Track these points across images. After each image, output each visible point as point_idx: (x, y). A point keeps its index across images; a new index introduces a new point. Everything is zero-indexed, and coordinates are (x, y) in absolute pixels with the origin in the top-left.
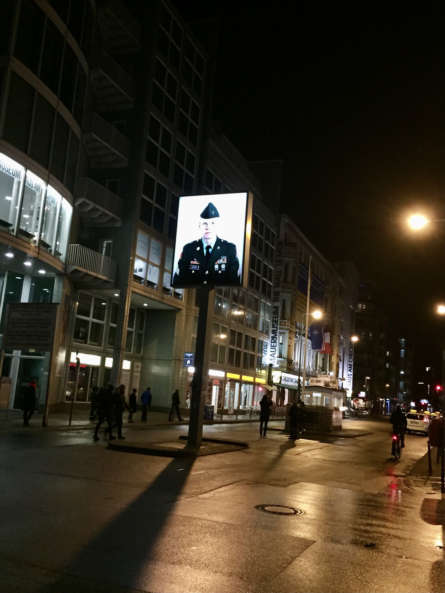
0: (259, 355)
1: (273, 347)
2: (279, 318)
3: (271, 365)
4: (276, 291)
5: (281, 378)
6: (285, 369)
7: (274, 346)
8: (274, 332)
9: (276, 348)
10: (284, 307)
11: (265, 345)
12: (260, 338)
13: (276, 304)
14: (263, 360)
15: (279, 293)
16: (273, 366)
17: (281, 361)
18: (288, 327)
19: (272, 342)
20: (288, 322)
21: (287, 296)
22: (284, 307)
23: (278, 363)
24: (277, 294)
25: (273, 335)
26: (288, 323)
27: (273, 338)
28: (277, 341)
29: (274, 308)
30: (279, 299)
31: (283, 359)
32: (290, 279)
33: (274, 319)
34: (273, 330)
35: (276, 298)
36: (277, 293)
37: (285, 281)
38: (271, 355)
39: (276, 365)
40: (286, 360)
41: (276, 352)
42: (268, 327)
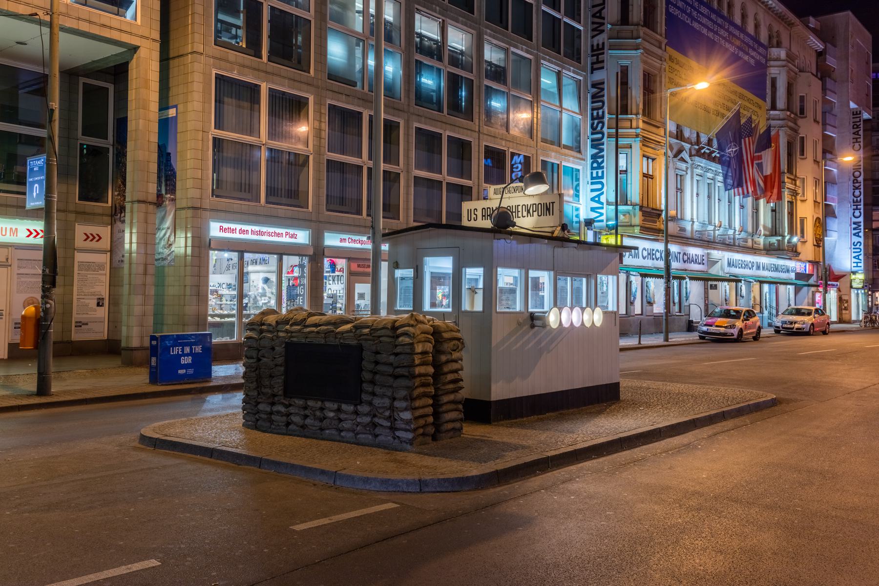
1: (596, 179)
2: (606, 108)
4: (595, 44)
6: (637, 230)
7: (598, 177)
9: (604, 181)
12: (547, 156)
13: (599, 76)
15: (603, 48)
18: (638, 131)
19: (593, 168)
20: (638, 119)
24: (597, 51)
25: (595, 151)
26: (639, 121)
28: (604, 164)
29: (594, 85)
30: (603, 61)
31: (630, 208)
34: (593, 140)
35: (598, 62)
36: (598, 49)
37: (624, 19)
38: (593, 199)
40: (637, 208)
41: (604, 190)
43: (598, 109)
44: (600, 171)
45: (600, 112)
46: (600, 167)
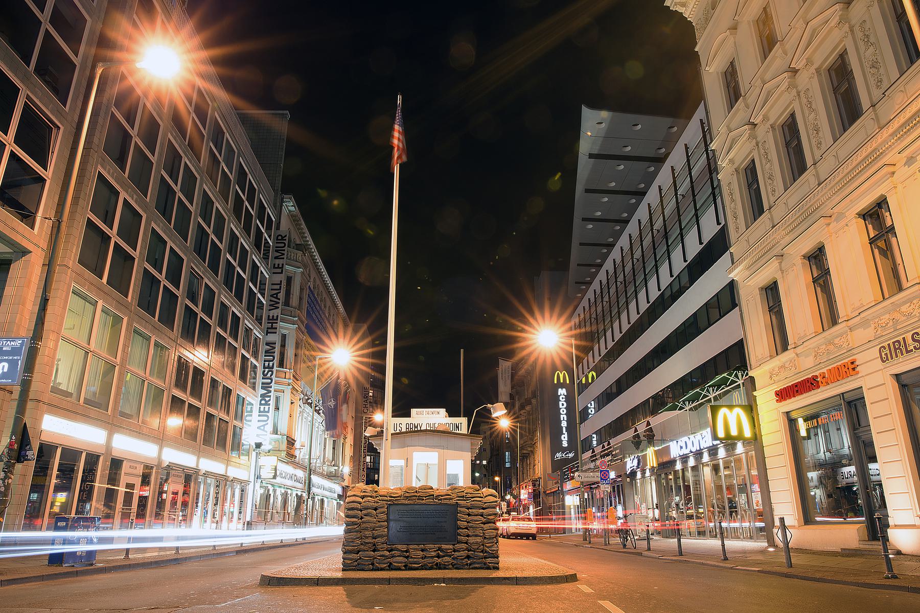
0: (237, 423)
3: (258, 445)
5: (276, 470)
6: (284, 454)
7: (264, 411)
8: (266, 386)
10: (283, 346)
11: (249, 409)
12: (240, 390)
13: (271, 338)
14: (243, 437)
16: (262, 447)
17: (276, 441)
18: (291, 381)
19: (261, 404)
21: (288, 328)
22: (283, 346)
23: (270, 444)
24: (273, 320)
27: (263, 396)
29: (267, 344)
32: (294, 301)
33: (267, 364)
35: (272, 328)
39: (266, 447)
42: (255, 378)
43: (269, 361)
44: (267, 407)
45: (271, 364)
46: (267, 403)
